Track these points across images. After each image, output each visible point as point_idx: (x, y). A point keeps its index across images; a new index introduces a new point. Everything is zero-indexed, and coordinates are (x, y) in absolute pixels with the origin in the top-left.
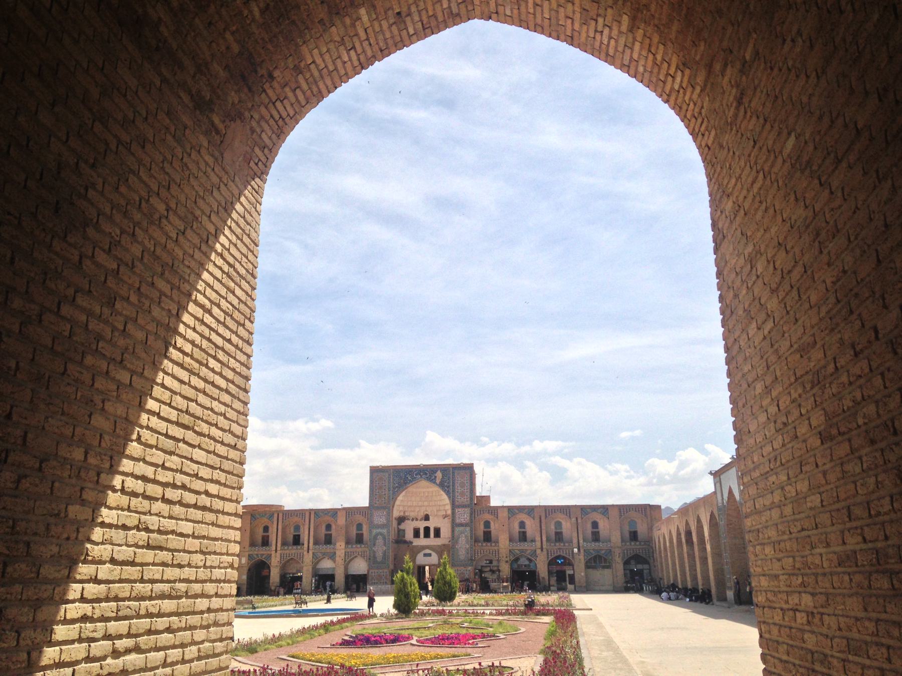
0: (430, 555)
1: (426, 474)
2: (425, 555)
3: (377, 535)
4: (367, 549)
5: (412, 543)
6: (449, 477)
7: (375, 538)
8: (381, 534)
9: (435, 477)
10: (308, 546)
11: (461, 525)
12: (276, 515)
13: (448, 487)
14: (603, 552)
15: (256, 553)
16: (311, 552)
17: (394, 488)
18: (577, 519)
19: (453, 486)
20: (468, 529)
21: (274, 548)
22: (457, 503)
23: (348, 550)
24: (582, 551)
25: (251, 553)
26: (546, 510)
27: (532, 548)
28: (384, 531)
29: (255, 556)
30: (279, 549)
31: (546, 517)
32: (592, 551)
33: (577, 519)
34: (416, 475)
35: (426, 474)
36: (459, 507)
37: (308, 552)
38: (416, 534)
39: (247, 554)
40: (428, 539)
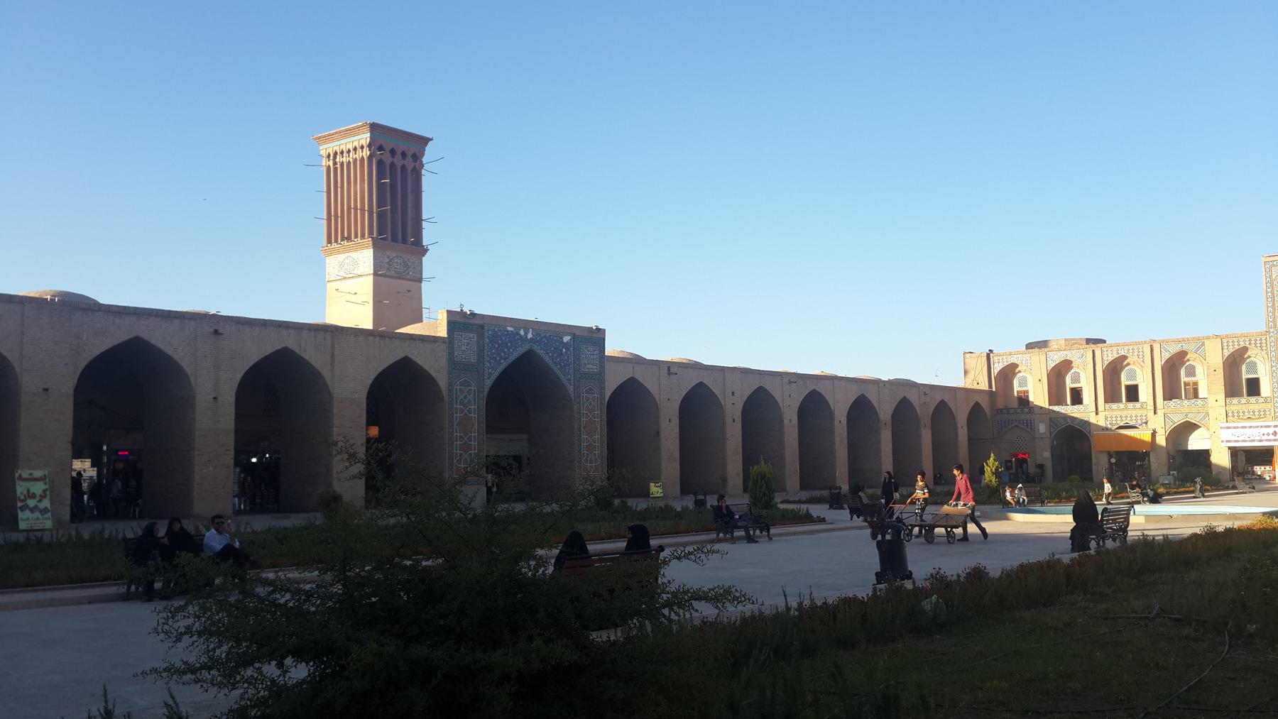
16: (1160, 412)
30: (1101, 408)
37: (1155, 413)
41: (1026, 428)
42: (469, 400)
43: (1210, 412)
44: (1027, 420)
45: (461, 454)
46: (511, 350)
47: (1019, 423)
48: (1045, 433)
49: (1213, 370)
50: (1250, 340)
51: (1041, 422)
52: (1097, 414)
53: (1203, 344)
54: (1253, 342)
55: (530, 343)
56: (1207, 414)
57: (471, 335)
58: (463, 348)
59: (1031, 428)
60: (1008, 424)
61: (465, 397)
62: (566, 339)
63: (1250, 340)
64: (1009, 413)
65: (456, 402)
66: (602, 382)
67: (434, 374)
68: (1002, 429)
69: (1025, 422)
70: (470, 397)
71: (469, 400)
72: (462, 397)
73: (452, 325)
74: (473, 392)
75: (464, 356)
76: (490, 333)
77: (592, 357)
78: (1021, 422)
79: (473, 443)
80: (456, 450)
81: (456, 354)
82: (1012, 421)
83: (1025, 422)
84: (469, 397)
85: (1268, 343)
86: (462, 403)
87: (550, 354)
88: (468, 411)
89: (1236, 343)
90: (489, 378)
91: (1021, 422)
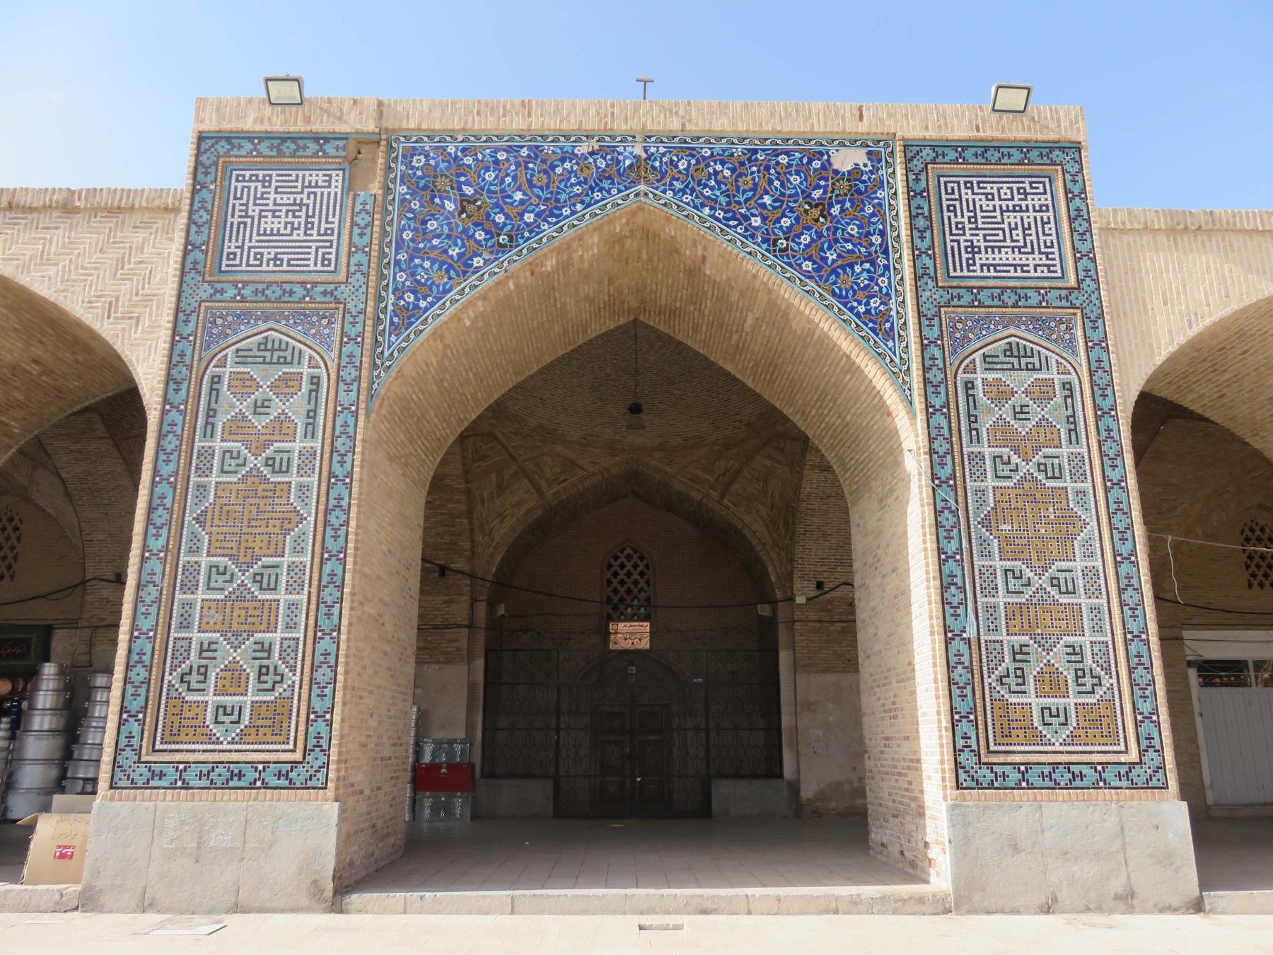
42: (283, 419)
45: (207, 649)
46: (529, 218)
55: (634, 183)
57: (317, 177)
58: (269, 223)
61: (260, 407)
62: (845, 160)
65: (210, 425)
66: (1095, 320)
67: (108, 330)
70: (296, 407)
71: (283, 419)
72: (245, 407)
73: (222, 147)
74: (305, 387)
75: (268, 254)
76: (419, 161)
77: (1012, 218)
79: (282, 596)
80: (185, 625)
81: (231, 246)
84: (277, 407)
86: (237, 427)
87: (756, 222)
88: (269, 462)
90: (395, 329)
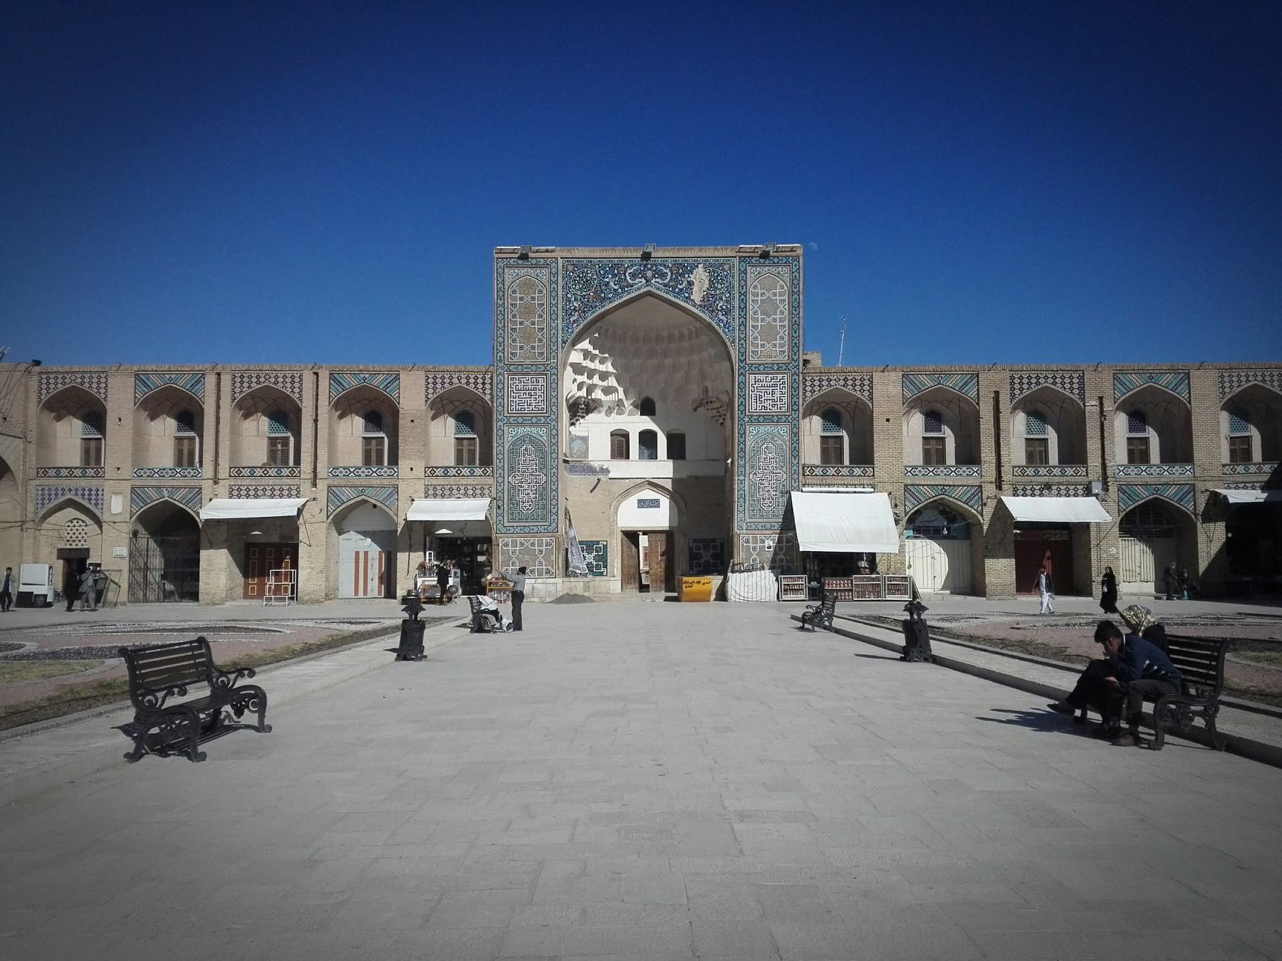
0: (655, 504)
1: (663, 275)
2: (642, 504)
3: (523, 439)
4: (490, 481)
5: (608, 471)
6: (730, 289)
7: (513, 451)
8: (533, 440)
9: (691, 284)
10: (315, 471)
11: (767, 419)
12: (210, 380)
13: (727, 312)
14: (1172, 490)
15: (154, 483)
16: (322, 485)
17: (568, 313)
18: (1101, 399)
19: (743, 308)
20: (784, 430)
21: (208, 470)
22: (752, 359)
23: (435, 482)
24: (1113, 489)
25: (139, 482)
26: (1012, 378)
27: (971, 481)
28: (541, 433)
29: (152, 493)
31: (1013, 395)
32: (1140, 490)
33: (1101, 399)
34: (634, 276)
35: (663, 275)
36: (757, 369)
38: (620, 446)
39: (126, 487)
40: (652, 463)
41: (88, 505)
43: (402, 487)
44: (90, 490)
47: (77, 494)
48: (121, 514)
49: (409, 419)
50: (468, 378)
51: (116, 493)
52: (216, 483)
53: (397, 378)
54: (472, 381)
56: (396, 488)
59: (96, 505)
60: (56, 495)
63: (468, 378)
64: (58, 476)
68: (43, 504)
69: (87, 492)
78: (80, 492)
82: (63, 490)
83: (87, 492)
85: (495, 384)
89: (447, 381)
91: (80, 492)
